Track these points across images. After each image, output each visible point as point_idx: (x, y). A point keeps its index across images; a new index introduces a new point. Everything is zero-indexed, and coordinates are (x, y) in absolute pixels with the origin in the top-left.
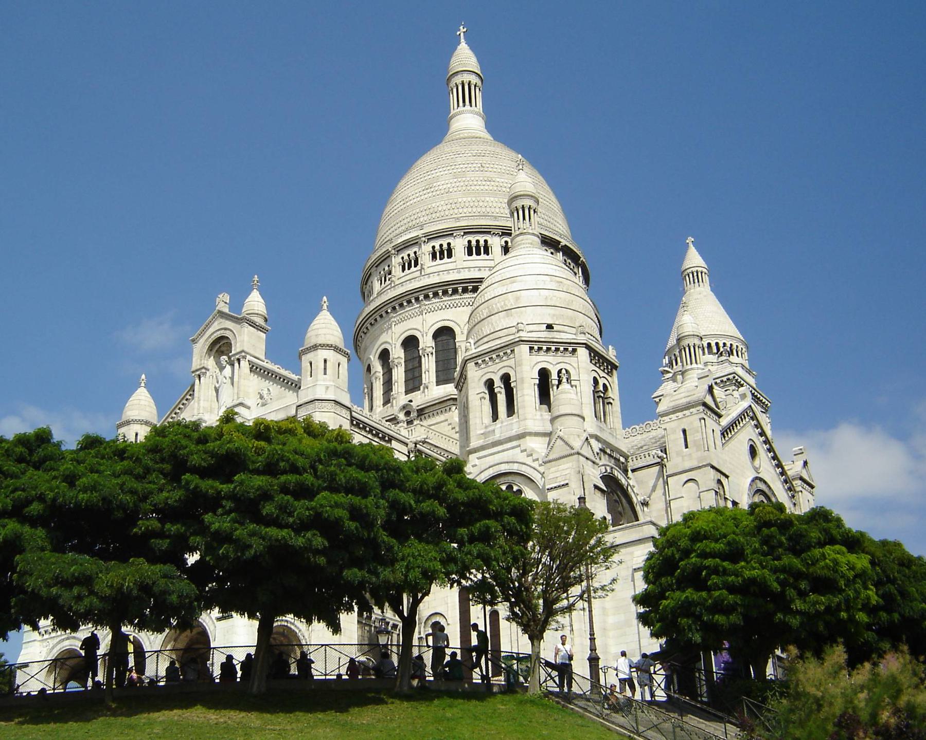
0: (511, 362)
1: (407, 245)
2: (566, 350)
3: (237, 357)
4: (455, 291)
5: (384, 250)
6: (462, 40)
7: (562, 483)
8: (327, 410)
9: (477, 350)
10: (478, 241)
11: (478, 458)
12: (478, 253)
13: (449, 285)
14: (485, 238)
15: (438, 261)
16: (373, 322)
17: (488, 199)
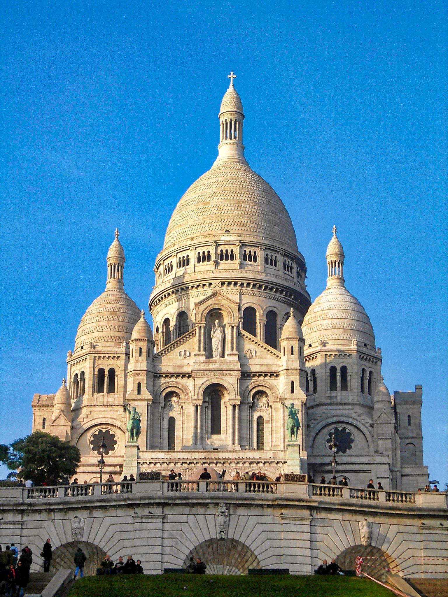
0: (350, 360)
1: (227, 243)
2: (373, 360)
4: (261, 286)
5: (207, 239)
6: (231, 84)
7: (388, 438)
9: (326, 348)
10: (272, 256)
11: (326, 409)
12: (271, 264)
13: (258, 281)
14: (275, 255)
15: (247, 262)
16: (195, 286)
17: (275, 227)
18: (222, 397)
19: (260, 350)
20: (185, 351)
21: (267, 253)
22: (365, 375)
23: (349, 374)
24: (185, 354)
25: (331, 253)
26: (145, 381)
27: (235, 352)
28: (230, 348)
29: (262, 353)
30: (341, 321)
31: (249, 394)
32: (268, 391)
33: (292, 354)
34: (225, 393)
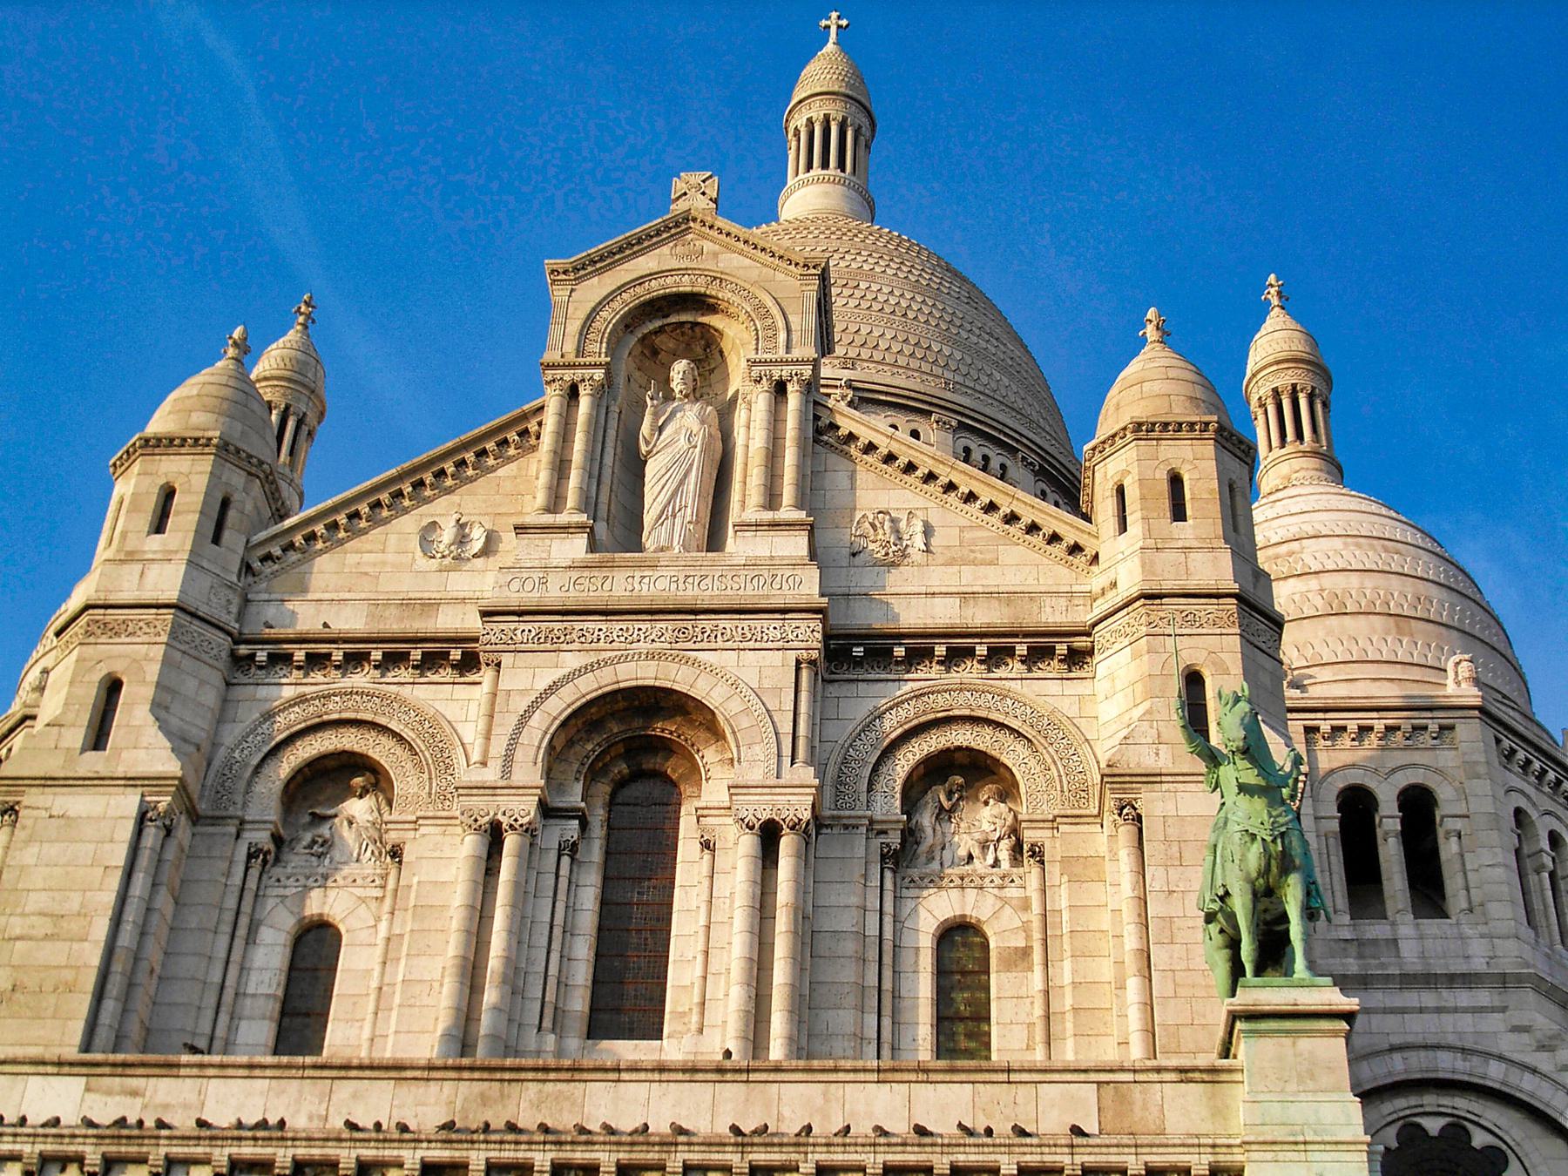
0: (1446, 758)
3: (777, 373)
8: (1264, 646)
10: (986, 458)
17: (997, 376)
18: (686, 789)
19: (952, 519)
20: (461, 526)
21: (963, 442)
22: (1526, 850)
23: (1450, 824)
24: (462, 539)
25: (1271, 359)
26: (153, 671)
27: (787, 513)
28: (755, 496)
29: (968, 535)
30: (1370, 581)
31: (875, 769)
32: (1011, 754)
33: (1179, 513)
34: (709, 756)
